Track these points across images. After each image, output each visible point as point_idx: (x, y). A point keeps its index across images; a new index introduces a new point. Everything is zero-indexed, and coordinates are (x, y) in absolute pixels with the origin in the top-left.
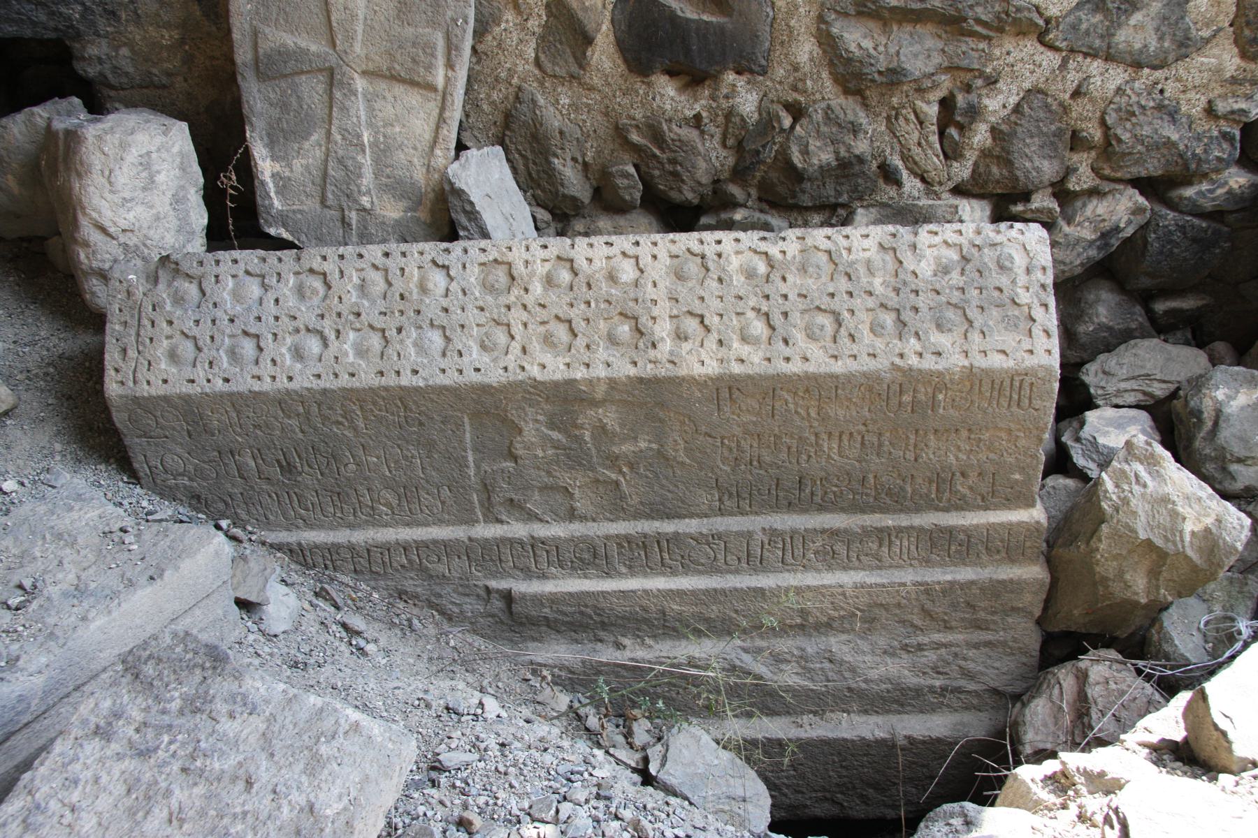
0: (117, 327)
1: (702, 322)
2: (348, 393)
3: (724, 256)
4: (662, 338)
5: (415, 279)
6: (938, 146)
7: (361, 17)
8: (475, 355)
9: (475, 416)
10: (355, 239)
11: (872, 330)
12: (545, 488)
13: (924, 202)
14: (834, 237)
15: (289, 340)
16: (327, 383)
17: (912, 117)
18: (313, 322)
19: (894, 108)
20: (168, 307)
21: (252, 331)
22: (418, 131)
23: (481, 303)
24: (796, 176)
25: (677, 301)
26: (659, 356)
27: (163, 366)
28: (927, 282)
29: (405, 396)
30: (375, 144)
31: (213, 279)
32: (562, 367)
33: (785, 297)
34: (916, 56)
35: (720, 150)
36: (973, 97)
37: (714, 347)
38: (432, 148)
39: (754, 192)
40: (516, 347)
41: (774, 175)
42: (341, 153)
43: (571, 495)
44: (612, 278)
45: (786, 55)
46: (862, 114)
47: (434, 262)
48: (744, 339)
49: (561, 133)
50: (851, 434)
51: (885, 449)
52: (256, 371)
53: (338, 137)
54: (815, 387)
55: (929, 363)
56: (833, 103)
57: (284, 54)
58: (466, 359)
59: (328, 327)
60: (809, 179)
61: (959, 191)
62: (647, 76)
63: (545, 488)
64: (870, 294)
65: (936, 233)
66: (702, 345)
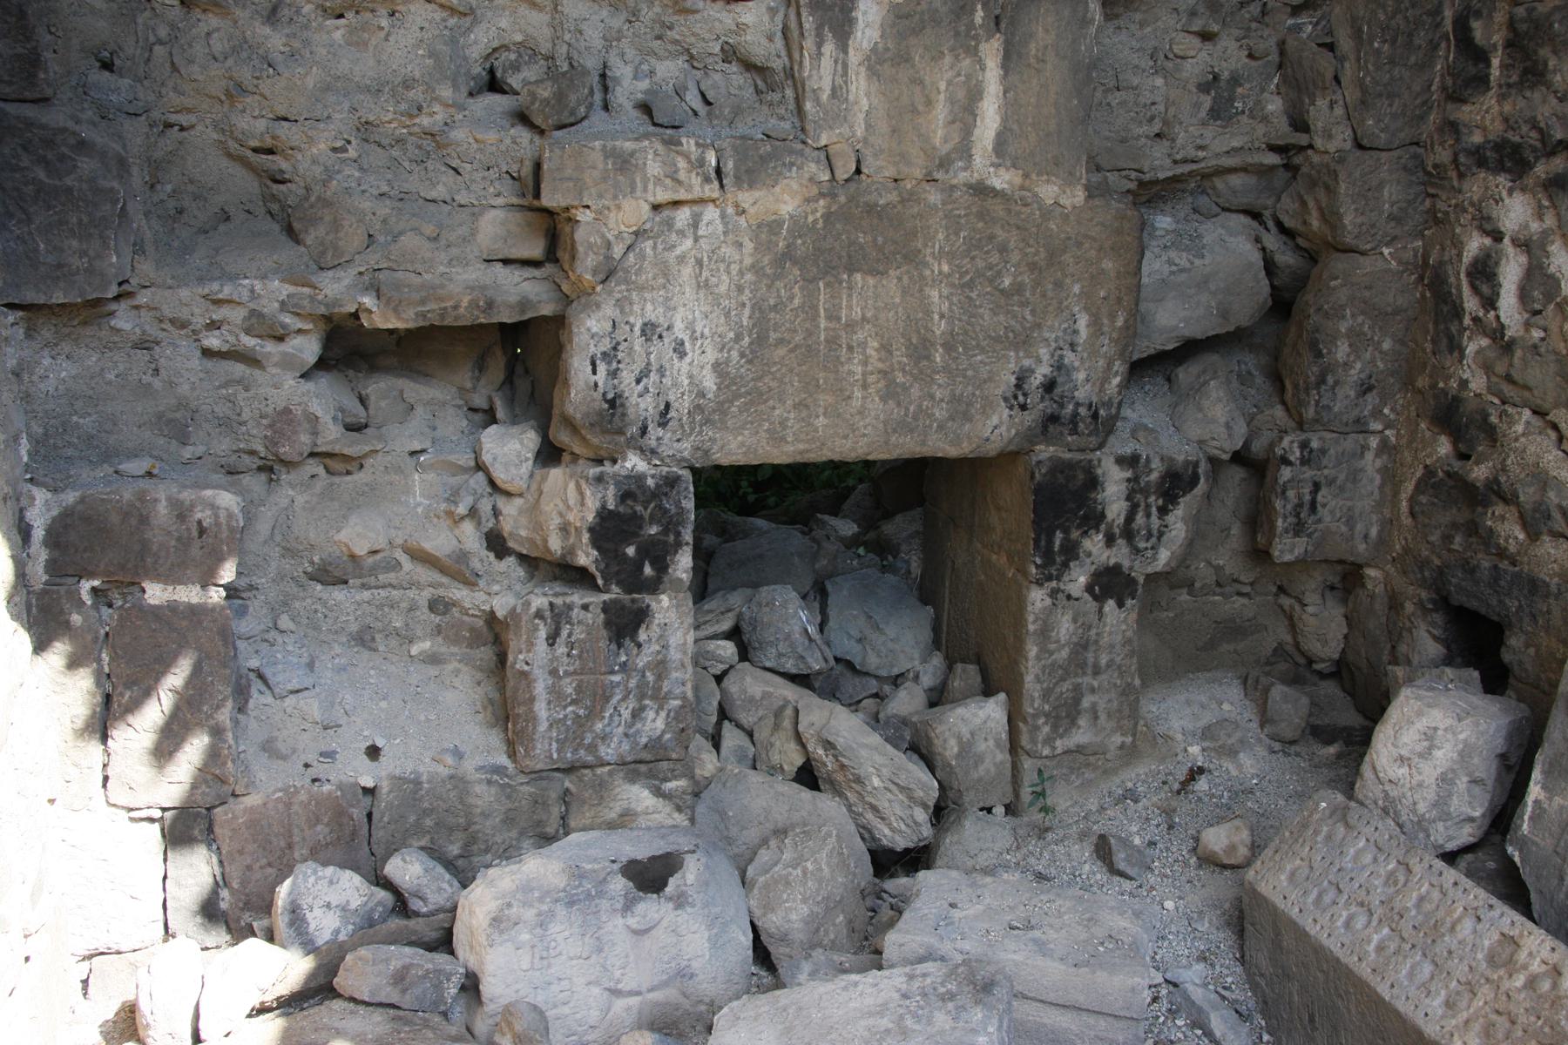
2: (1349, 973)
8: (1436, 1004)
29: (1377, 1002)
40: (1465, 1015)
52: (1318, 916)
58: (1427, 1001)
59: (1379, 911)
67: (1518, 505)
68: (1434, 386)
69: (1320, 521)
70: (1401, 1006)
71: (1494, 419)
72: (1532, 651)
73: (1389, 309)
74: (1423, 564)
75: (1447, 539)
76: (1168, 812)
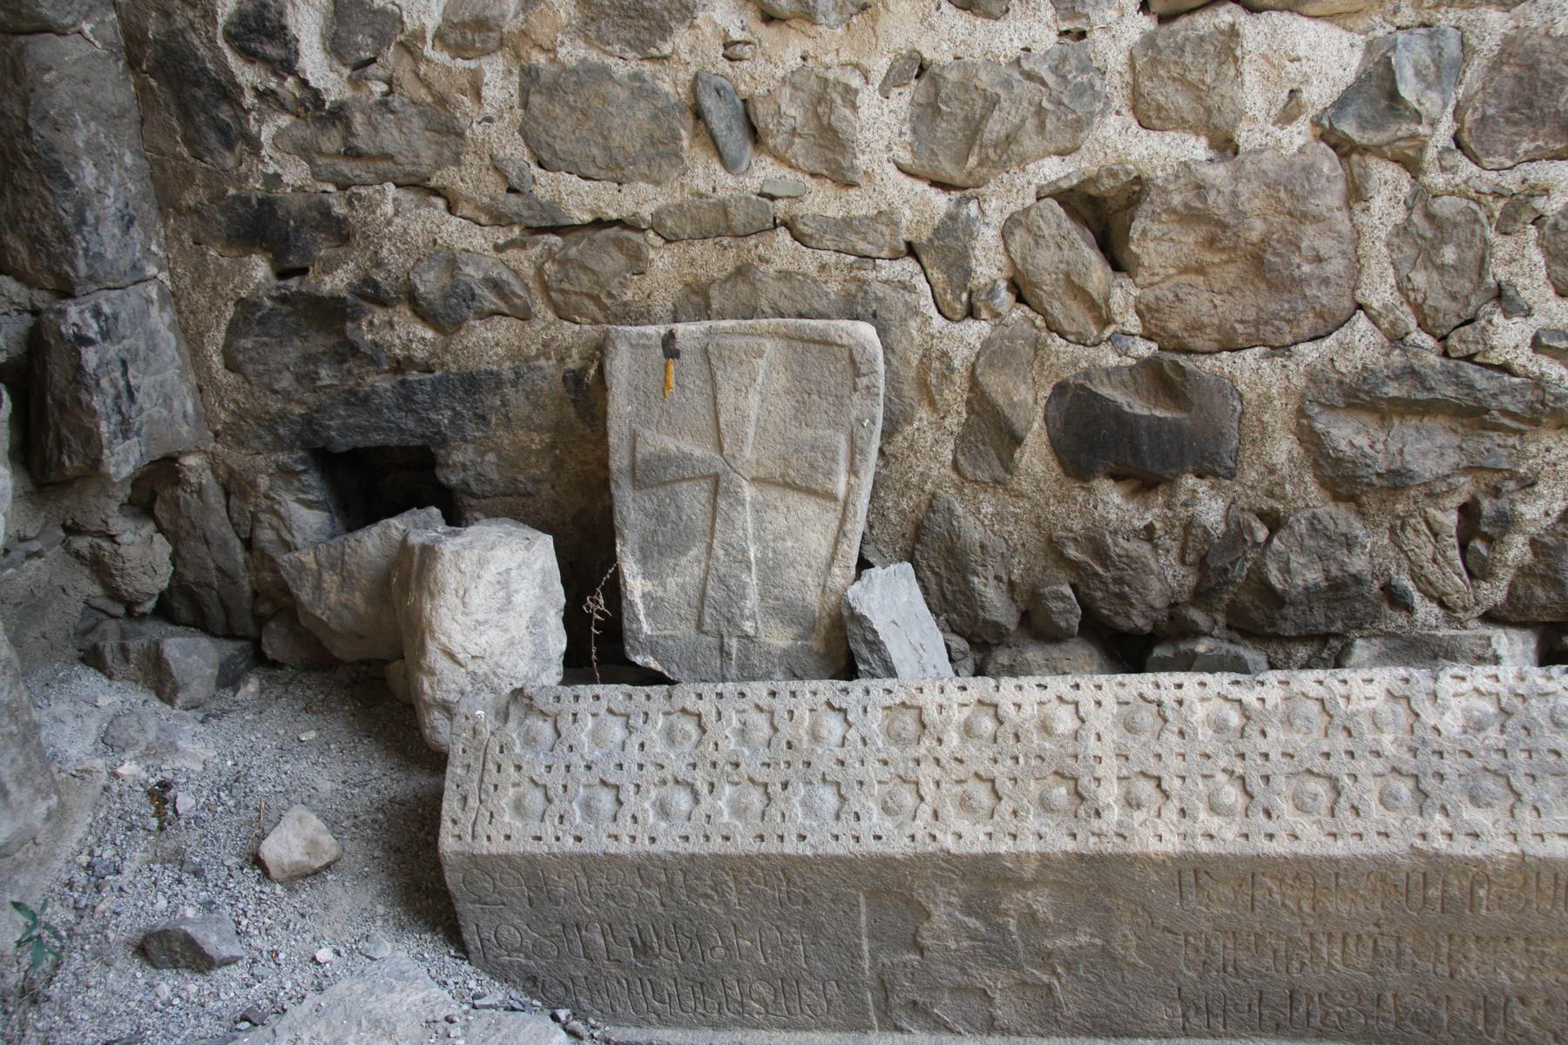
0: (459, 771)
1: (1159, 786)
2: (720, 860)
3: (1186, 703)
4: (1109, 806)
5: (806, 724)
6: (1459, 562)
7: (753, 417)
8: (875, 819)
9: (874, 895)
10: (734, 671)
11: (1382, 802)
12: (957, 990)
13: (1444, 632)
14: (1327, 682)
15: (653, 794)
16: (696, 847)
17: (1424, 527)
18: (683, 772)
19: (1398, 517)
20: (517, 750)
21: (612, 780)
22: (813, 547)
23: (884, 756)
24: (1276, 599)
25: (1127, 758)
26: (1105, 828)
27: (507, 819)
28: (1455, 741)
30: (762, 561)
31: (571, 718)
32: (982, 837)
33: (1266, 756)
34: (1424, 454)
35: (1178, 567)
36: (1503, 503)
37: (1175, 818)
38: (829, 566)
39: (1221, 618)
40: (925, 811)
41: (1246, 598)
42: (723, 570)
43: (991, 1000)
44: (1045, 728)
45: (1259, 455)
46: (1357, 524)
47: (829, 704)
48: (1214, 809)
49: (982, 547)
50: (1359, 937)
51: (1407, 958)
52: (613, 829)
53: (721, 553)
54: (1306, 873)
55: (1462, 847)
56: (1317, 511)
57: (664, 459)
58: (864, 823)
59: (700, 780)
60: (1292, 604)
61: (1491, 617)
62: (1087, 481)
63: (957, 990)
64: (1378, 754)
65: (1463, 679)
66: (1159, 815)
67: (412, 298)
68: (218, 197)
69: (141, 410)
70: (834, 848)
71: (339, 209)
72: (491, 457)
73: (115, 110)
74: (270, 423)
75: (307, 379)
76: (178, 859)
